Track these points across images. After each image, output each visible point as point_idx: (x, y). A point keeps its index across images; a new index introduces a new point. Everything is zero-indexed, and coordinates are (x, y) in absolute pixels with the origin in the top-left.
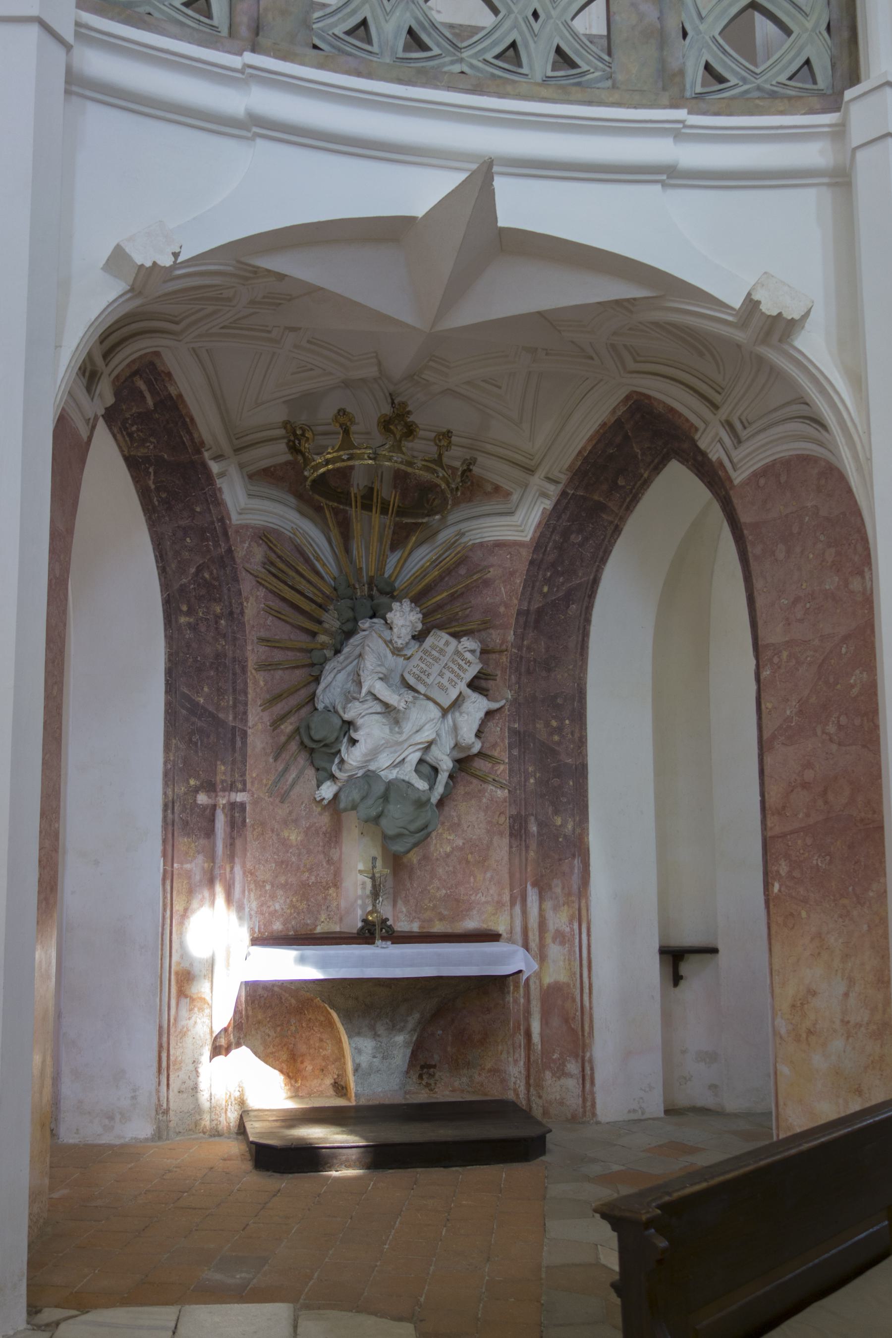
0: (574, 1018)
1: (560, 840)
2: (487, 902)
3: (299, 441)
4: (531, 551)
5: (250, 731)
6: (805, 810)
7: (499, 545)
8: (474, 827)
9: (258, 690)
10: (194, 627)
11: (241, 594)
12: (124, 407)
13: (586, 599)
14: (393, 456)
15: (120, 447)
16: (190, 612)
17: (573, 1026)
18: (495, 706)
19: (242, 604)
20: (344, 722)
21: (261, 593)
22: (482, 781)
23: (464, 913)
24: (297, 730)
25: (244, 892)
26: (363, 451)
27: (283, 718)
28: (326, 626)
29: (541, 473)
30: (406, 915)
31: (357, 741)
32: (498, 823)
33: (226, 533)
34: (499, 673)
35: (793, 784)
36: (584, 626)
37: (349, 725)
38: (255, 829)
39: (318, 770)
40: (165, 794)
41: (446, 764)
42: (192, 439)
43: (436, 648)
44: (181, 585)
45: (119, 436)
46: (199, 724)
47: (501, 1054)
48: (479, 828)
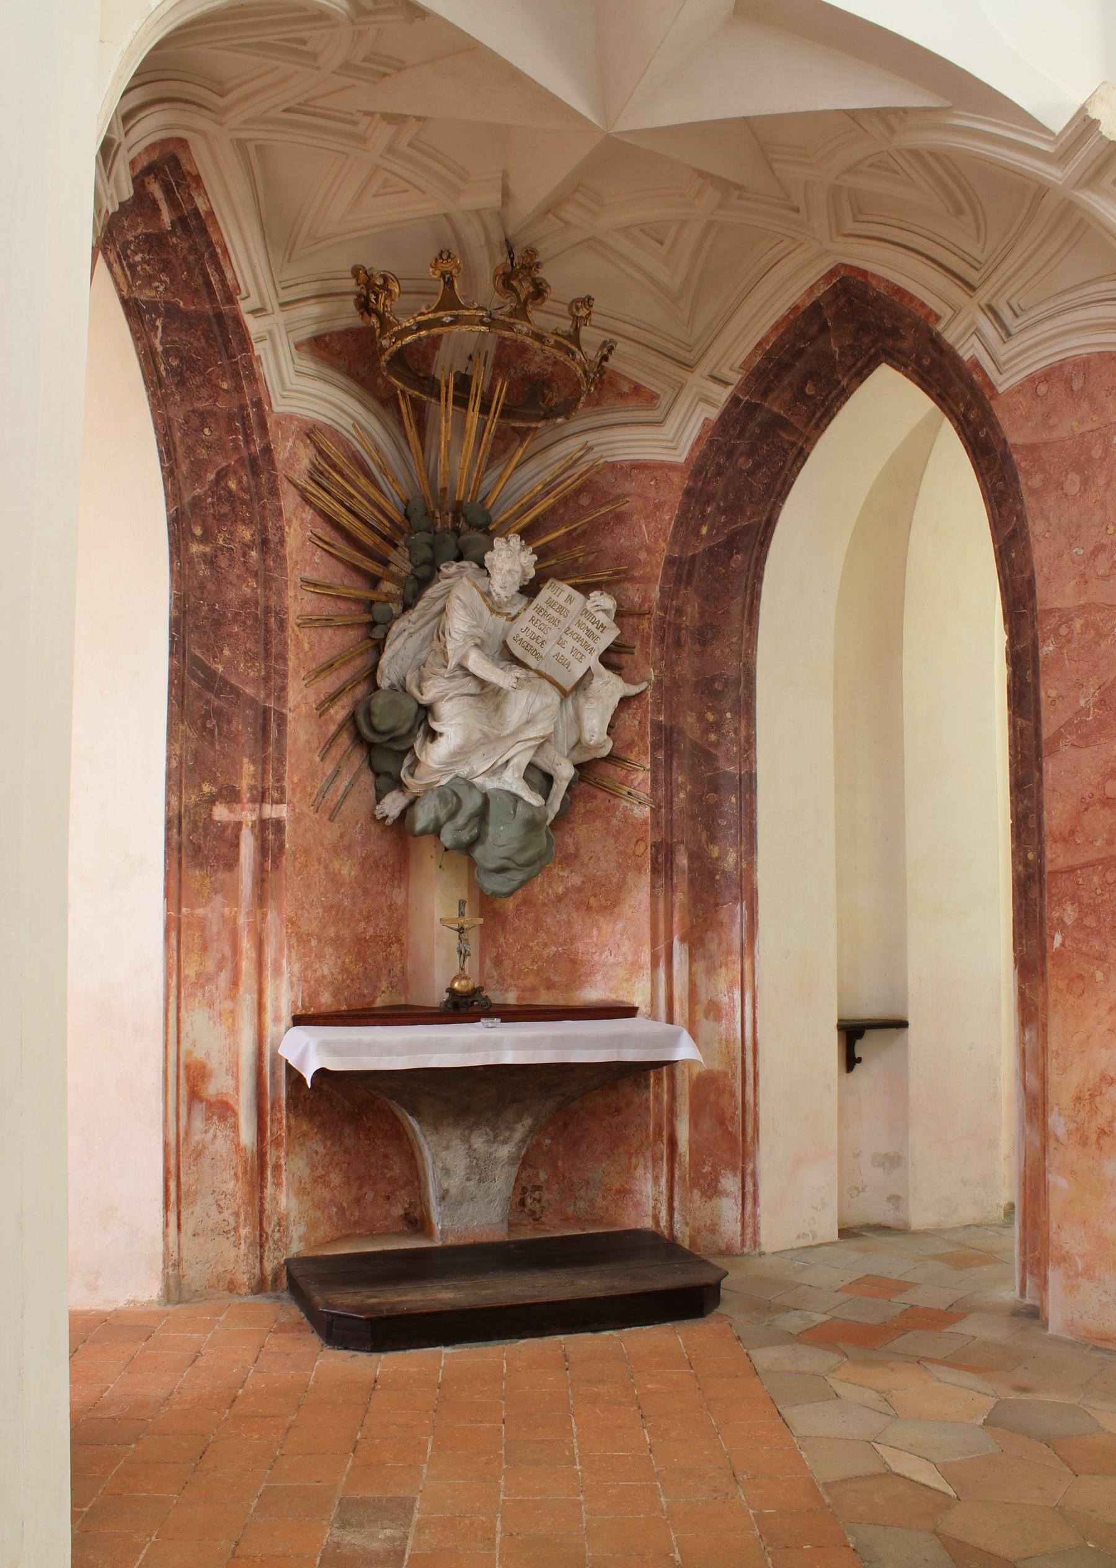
0: (733, 1118)
1: (717, 877)
2: (618, 964)
3: (377, 295)
4: (687, 477)
5: (290, 716)
6: (1105, 836)
8: (599, 859)
9: (301, 656)
10: (210, 561)
11: (281, 514)
12: (126, 224)
13: (757, 547)
14: (514, 323)
15: (117, 284)
16: (205, 538)
17: (730, 1129)
18: (633, 690)
19: (281, 528)
20: (420, 706)
21: (308, 514)
22: (612, 794)
23: (583, 978)
24: (352, 718)
25: (281, 949)
26: (473, 312)
28: (393, 568)
29: (705, 367)
30: (497, 982)
31: (441, 734)
32: (634, 854)
33: (263, 425)
34: (638, 644)
35: (1088, 800)
36: (754, 585)
37: (426, 711)
38: (296, 859)
39: (377, 775)
40: (168, 804)
41: (565, 772)
42: (223, 280)
43: (555, 605)
44: (194, 498)
45: (117, 268)
46: (217, 703)
47: (635, 1169)
48: (607, 861)
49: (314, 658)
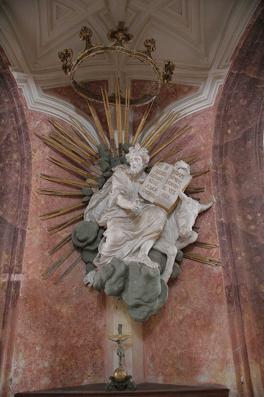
2: (214, 360)
5: (28, 232)
7: (195, 115)
13: (257, 135)
18: (205, 207)
21: (47, 150)
23: (196, 369)
27: (61, 227)
33: (23, 114)
34: (205, 187)
38: (28, 302)
39: (86, 263)
49: (48, 208)
